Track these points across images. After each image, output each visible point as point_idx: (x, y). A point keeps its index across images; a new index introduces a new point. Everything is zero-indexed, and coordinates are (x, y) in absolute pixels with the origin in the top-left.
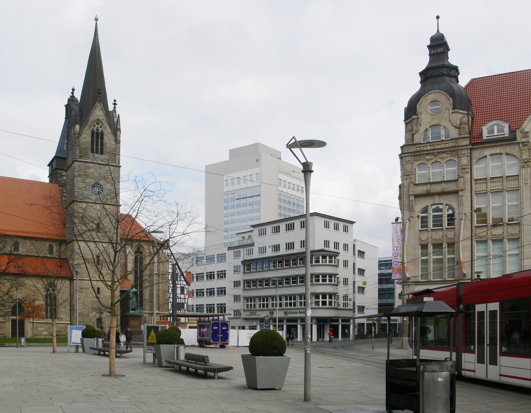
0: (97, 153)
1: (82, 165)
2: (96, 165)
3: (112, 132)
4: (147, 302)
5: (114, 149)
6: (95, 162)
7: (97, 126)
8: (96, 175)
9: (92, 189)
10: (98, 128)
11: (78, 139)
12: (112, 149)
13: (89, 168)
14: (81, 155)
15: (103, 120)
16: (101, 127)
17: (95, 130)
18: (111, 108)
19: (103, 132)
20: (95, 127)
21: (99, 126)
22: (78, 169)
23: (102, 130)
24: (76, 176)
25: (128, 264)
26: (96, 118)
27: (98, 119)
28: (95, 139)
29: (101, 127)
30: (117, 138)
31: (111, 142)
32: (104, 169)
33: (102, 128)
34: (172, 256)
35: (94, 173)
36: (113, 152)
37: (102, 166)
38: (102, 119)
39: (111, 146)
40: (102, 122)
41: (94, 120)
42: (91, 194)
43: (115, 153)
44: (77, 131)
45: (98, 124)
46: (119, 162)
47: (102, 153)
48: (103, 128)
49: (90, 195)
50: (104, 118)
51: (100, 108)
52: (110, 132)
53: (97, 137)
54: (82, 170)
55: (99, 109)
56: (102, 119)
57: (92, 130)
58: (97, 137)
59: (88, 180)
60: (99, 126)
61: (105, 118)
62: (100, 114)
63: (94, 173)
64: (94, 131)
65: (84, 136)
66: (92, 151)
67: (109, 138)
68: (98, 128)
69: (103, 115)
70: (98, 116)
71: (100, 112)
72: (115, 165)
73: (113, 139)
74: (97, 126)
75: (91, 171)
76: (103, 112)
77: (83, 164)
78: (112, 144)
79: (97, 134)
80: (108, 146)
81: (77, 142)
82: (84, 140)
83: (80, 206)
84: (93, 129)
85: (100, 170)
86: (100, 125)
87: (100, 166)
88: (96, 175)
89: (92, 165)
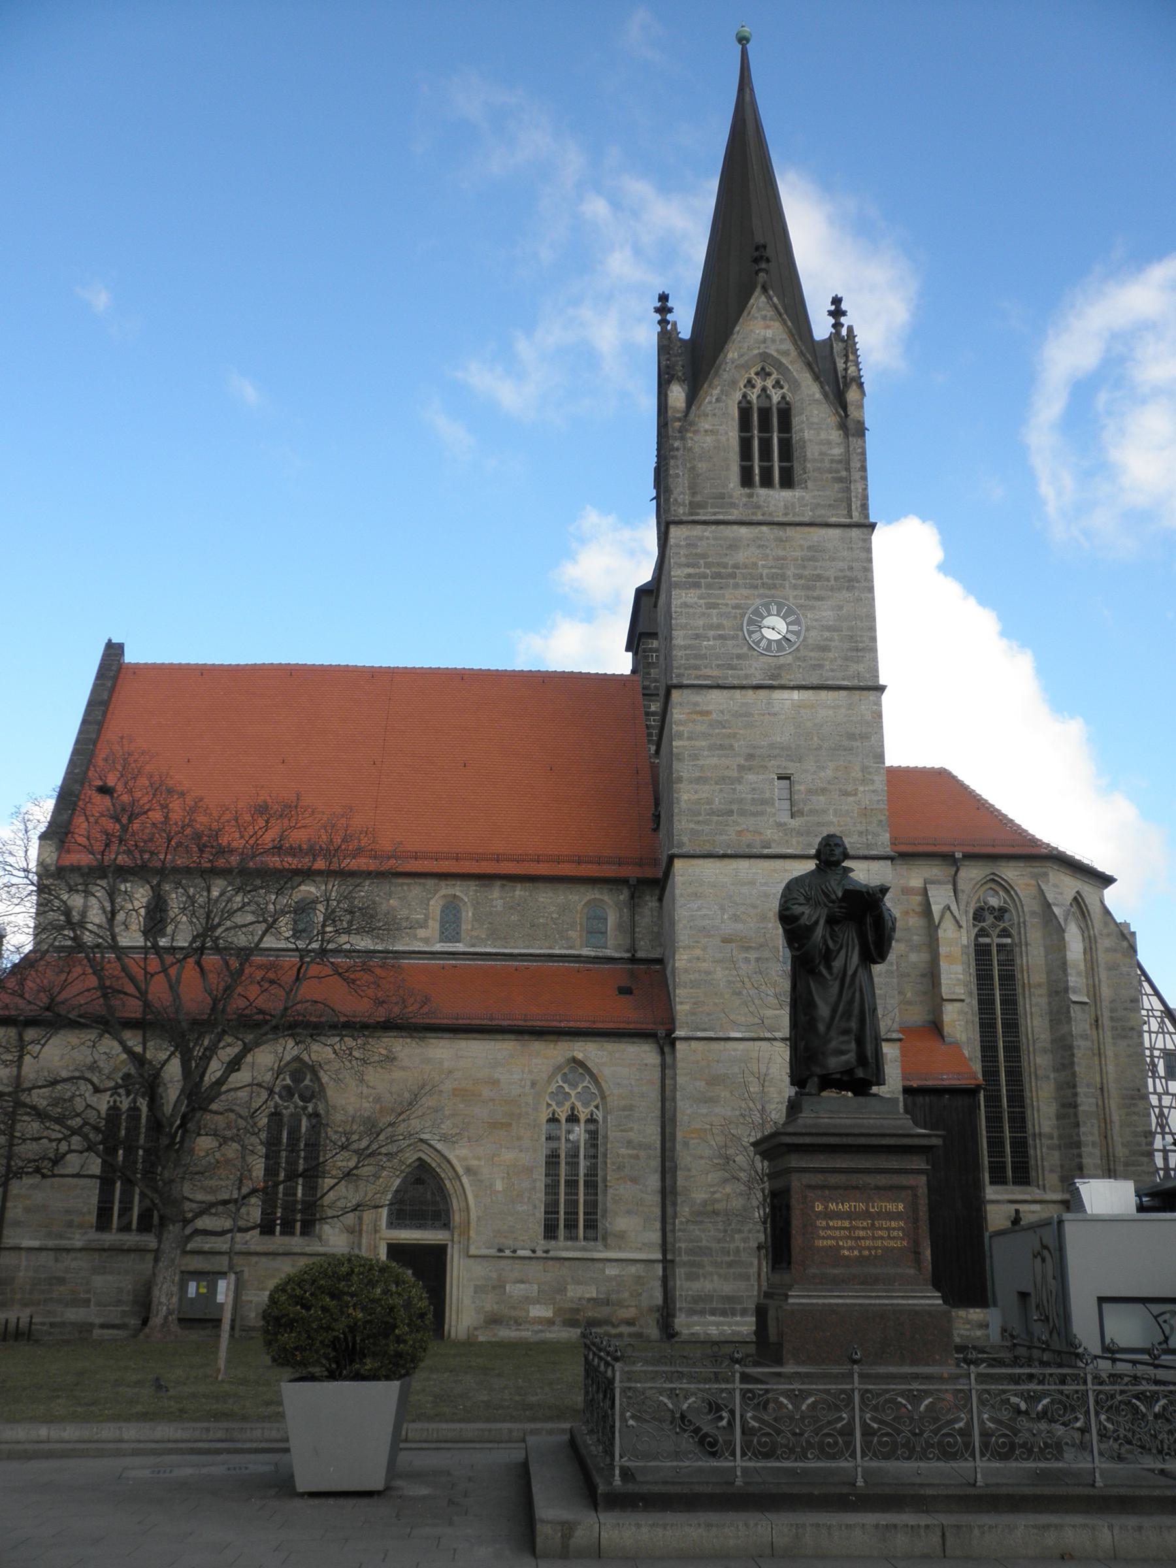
0: (767, 482)
1: (701, 539)
2: (764, 529)
3: (825, 395)
4: (1049, 1148)
5: (840, 462)
6: (760, 518)
7: (759, 383)
8: (765, 571)
9: (752, 628)
10: (764, 389)
11: (683, 439)
12: (832, 461)
13: (734, 546)
14: (698, 498)
15: (786, 353)
16: (778, 385)
17: (754, 397)
18: (822, 329)
19: (788, 403)
20: (753, 387)
21: (769, 383)
22: (686, 556)
23: (783, 397)
24: (677, 585)
25: (944, 966)
26: (756, 352)
27: (765, 356)
28: (756, 432)
29: (778, 385)
30: (847, 416)
31: (823, 436)
32: (802, 542)
33: (782, 388)
34: (1145, 984)
35: (755, 565)
36: (837, 471)
37: (790, 532)
38: (778, 351)
39: (824, 448)
40: (779, 366)
41: (746, 358)
42: (745, 649)
43: (844, 474)
44: (676, 410)
45: (764, 373)
46: (865, 507)
47: (788, 481)
48: (786, 387)
49: (739, 657)
50: (788, 346)
51: (770, 313)
52: (818, 396)
53: (765, 426)
54: (704, 556)
55: (764, 318)
56: (778, 351)
57: (740, 403)
58: (765, 426)
59: (730, 597)
60: (769, 383)
61: (792, 348)
62: (769, 333)
63: (755, 565)
64: (749, 402)
65: (707, 427)
66: (746, 479)
67: (816, 420)
68: (764, 389)
69: (785, 336)
70: (764, 341)
71: (768, 327)
72: (848, 521)
73: (833, 420)
74: (759, 383)
75: (741, 557)
76: (784, 323)
77: (706, 534)
78: (829, 443)
79: (765, 413)
80: (812, 451)
81: (677, 449)
82: (709, 439)
83: (696, 704)
84: (745, 396)
85: (785, 549)
86: (775, 376)
87: (778, 532)
88: (765, 571)
89: (743, 531)
